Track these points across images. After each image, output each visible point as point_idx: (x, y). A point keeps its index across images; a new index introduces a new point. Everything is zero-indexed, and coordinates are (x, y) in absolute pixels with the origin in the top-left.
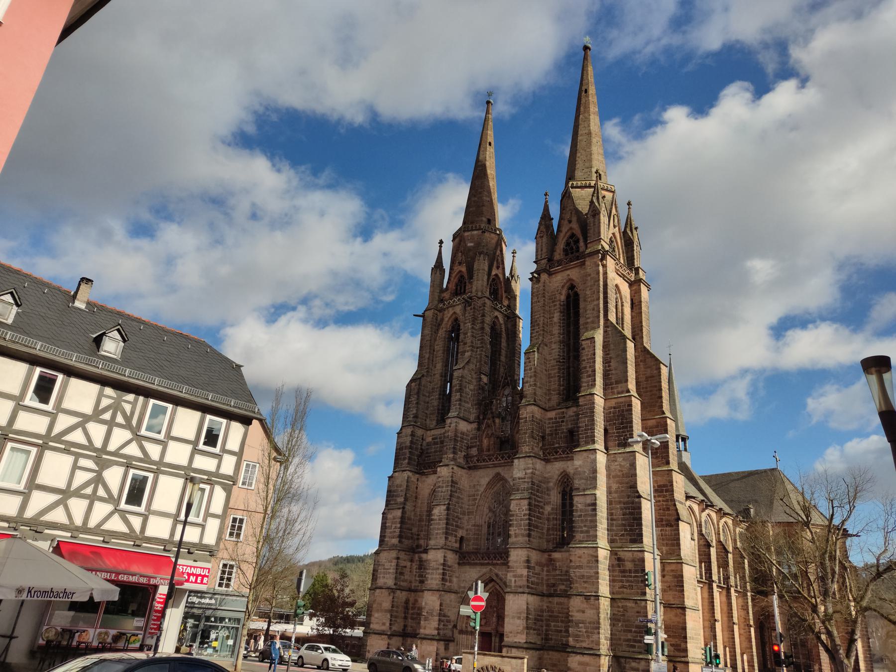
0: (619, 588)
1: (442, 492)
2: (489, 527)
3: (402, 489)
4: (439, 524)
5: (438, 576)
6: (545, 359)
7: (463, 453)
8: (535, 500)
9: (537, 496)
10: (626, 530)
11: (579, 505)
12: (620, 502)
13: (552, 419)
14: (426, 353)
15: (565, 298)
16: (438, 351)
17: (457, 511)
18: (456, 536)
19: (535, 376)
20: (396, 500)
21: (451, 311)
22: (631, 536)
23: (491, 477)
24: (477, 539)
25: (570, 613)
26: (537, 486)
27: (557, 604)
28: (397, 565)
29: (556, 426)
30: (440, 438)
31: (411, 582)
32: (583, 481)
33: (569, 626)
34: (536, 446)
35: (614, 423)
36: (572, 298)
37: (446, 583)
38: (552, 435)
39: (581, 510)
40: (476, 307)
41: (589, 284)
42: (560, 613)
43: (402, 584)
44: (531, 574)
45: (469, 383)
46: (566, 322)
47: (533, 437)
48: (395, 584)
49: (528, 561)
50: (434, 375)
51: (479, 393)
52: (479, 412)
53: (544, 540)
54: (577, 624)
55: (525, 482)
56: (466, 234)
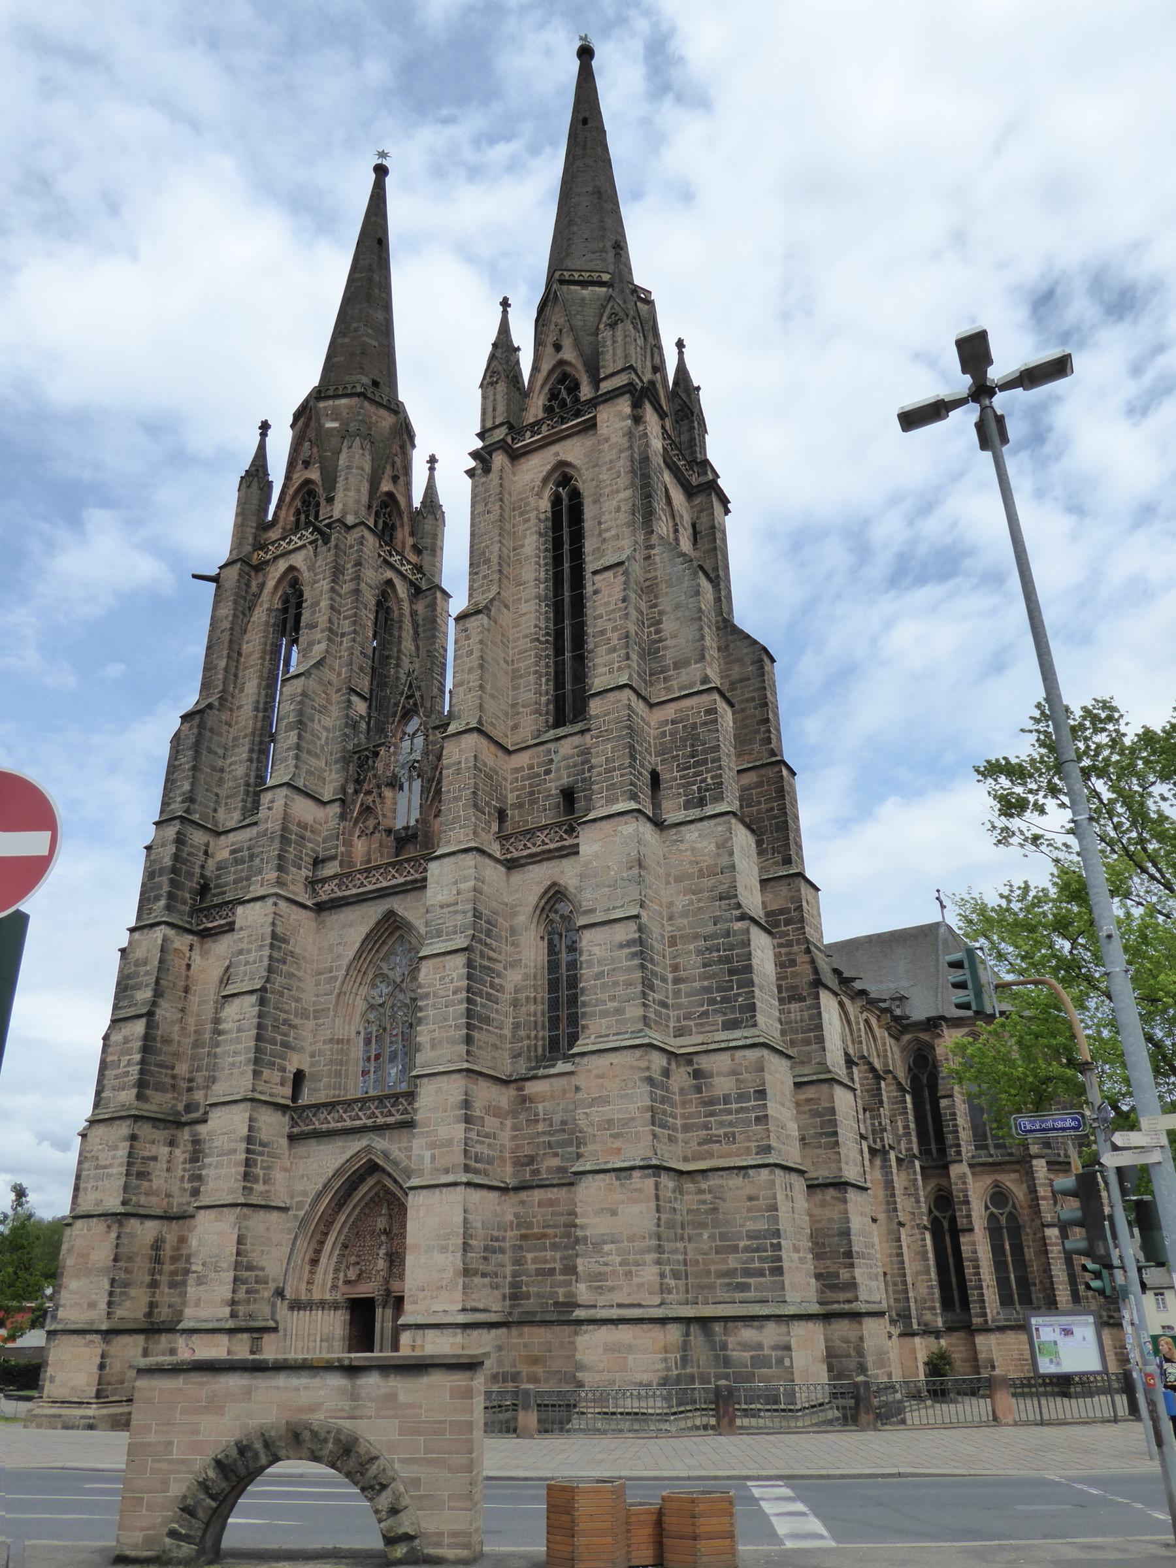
0: (699, 1144)
1: (247, 963)
2: (368, 1042)
3: (148, 968)
4: (238, 1041)
5: (233, 1170)
6: (503, 635)
7: (305, 872)
8: (482, 955)
9: (486, 944)
10: (712, 1002)
11: (596, 950)
12: (696, 937)
13: (521, 769)
14: (220, 657)
15: (549, 505)
17: (287, 1007)
18: (283, 1069)
19: (481, 667)
20: (132, 997)
21: (282, 565)
22: (725, 1014)
23: (371, 923)
24: (338, 1074)
25: (578, 1221)
26: (488, 922)
27: (539, 1205)
28: (130, 1155)
29: (531, 786)
30: (249, 849)
31: (168, 1196)
32: (605, 890)
33: (577, 1256)
34: (483, 829)
35: (673, 757)
36: (565, 502)
37: (255, 1186)
38: (520, 806)
39: (600, 962)
40: (343, 547)
41: (607, 459)
42: (549, 1226)
43: (143, 1200)
44: (473, 1135)
46: (550, 555)
47: (476, 806)
48: (124, 1203)
49: (467, 1104)
50: (240, 707)
51: (345, 734)
53: (506, 1055)
54: (597, 1246)
56: (322, 405)
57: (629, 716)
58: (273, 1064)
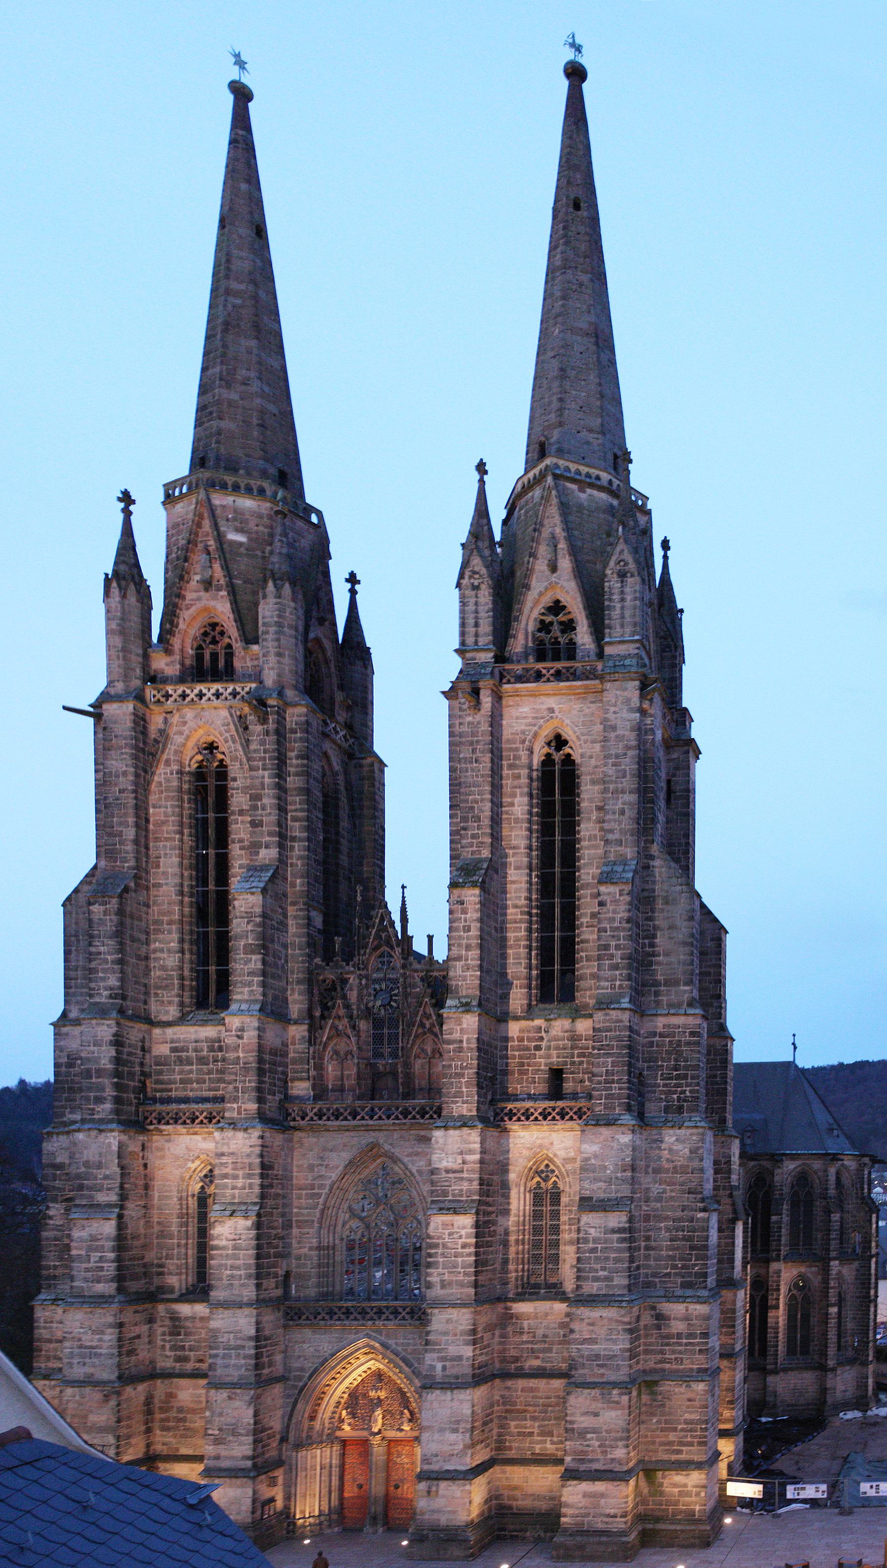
16: (164, 823)
30: (196, 1050)
45: (278, 929)
52: (311, 1002)
55: (462, 1179)
57: (630, 1037)
58: (269, 1274)
